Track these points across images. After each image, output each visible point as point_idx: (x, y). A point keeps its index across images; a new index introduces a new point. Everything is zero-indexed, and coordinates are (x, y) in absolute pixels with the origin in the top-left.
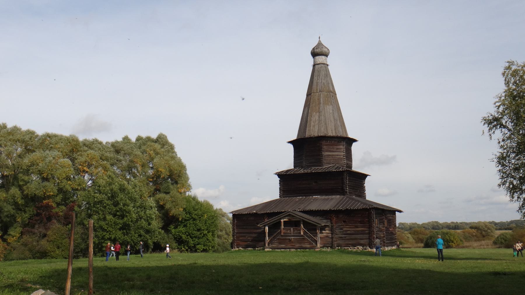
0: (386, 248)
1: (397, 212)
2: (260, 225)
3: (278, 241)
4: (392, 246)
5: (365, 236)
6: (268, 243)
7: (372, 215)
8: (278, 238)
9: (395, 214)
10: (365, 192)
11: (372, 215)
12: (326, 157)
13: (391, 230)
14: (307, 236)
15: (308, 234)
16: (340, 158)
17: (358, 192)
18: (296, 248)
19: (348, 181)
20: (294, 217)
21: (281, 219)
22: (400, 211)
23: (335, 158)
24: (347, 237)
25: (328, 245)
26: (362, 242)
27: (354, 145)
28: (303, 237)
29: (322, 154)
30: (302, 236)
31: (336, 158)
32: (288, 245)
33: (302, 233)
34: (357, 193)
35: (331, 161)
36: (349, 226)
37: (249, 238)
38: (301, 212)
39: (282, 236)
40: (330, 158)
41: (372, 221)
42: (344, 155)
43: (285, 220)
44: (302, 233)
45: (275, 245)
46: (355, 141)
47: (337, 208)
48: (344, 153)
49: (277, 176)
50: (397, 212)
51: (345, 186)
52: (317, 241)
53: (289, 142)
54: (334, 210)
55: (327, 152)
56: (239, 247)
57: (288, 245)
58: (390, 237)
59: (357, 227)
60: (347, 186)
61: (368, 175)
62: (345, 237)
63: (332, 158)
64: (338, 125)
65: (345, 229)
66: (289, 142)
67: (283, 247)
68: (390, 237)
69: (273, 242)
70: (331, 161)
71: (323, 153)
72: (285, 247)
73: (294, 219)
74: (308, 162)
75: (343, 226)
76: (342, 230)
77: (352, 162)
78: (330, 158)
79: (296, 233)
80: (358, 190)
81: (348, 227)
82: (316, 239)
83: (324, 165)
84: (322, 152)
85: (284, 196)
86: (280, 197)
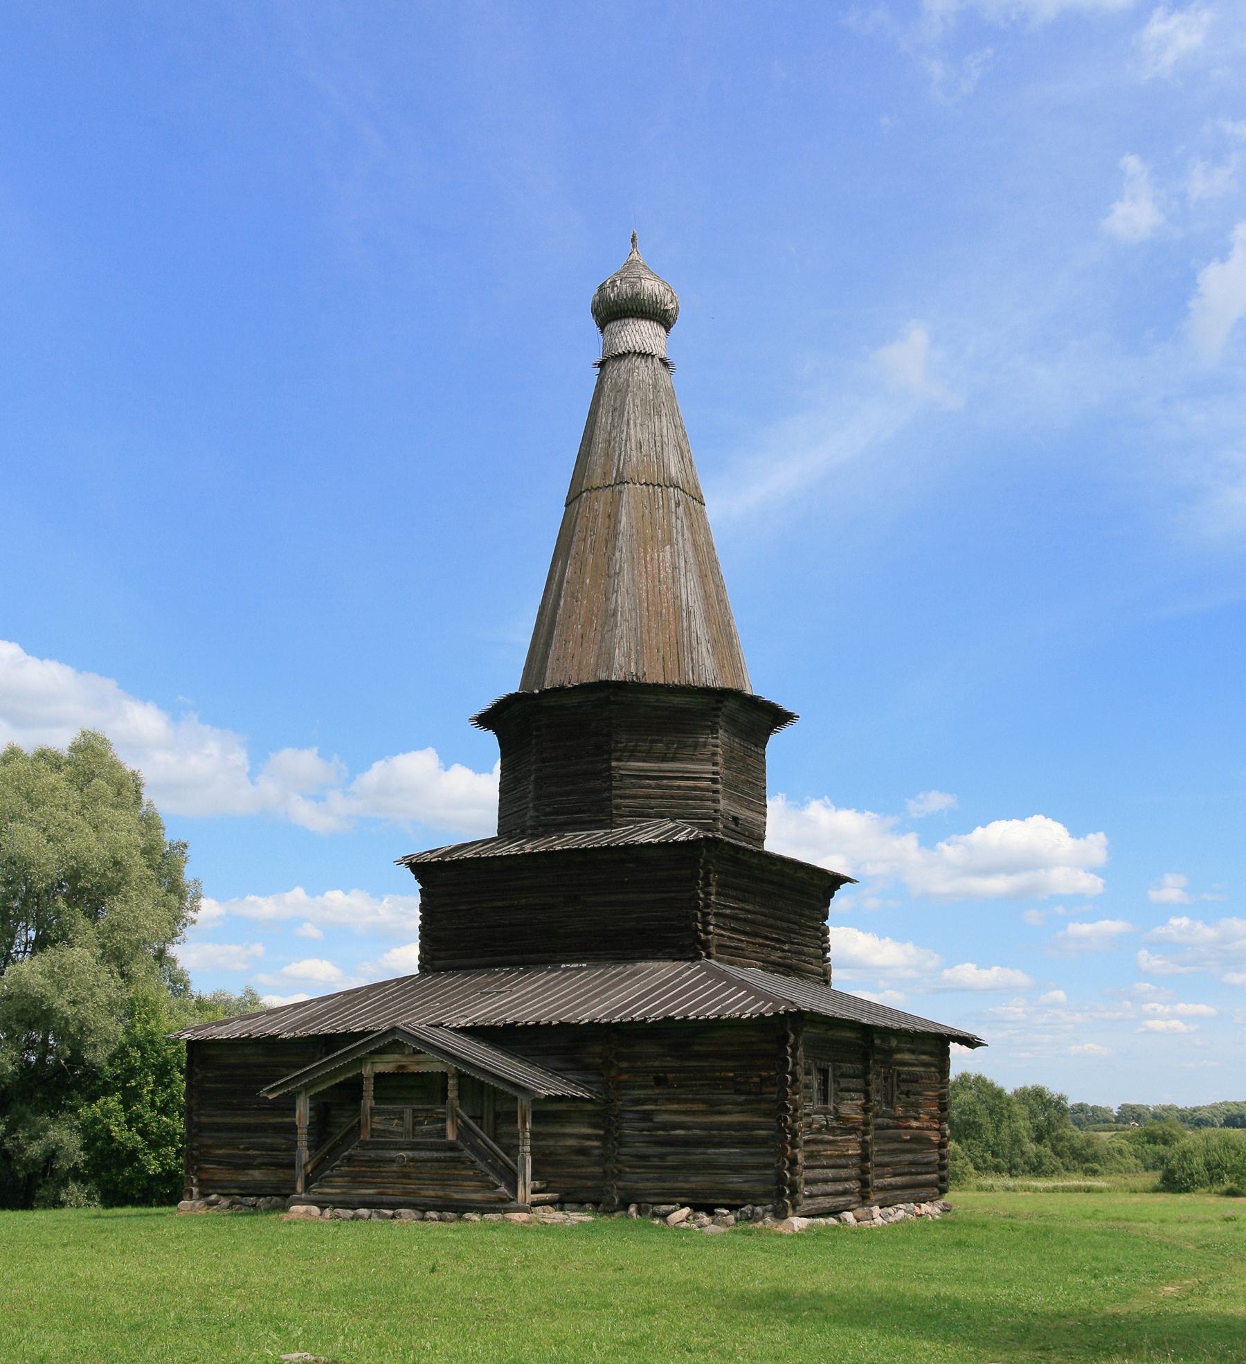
0: (876, 1210)
1: (954, 1048)
2: (271, 1091)
3: (347, 1169)
4: (920, 1201)
5: (753, 1154)
6: (307, 1176)
7: (789, 1050)
8: (346, 1153)
9: (944, 1054)
10: (828, 955)
11: (789, 1050)
12: (628, 781)
13: (914, 1124)
14: (474, 1149)
15: (479, 1136)
16: (695, 788)
17: (783, 951)
18: (425, 1205)
19: (713, 890)
20: (421, 1057)
21: (360, 1062)
22: (970, 1042)
23: (672, 787)
24: (670, 1158)
25: (581, 1196)
26: (736, 1181)
27: (778, 744)
28: (456, 1154)
29: (610, 768)
30: (452, 1147)
31: (679, 787)
32: (390, 1191)
33: (451, 1136)
34: (779, 954)
35: (653, 802)
36: (679, 1101)
37: (251, 1152)
38: (463, 1031)
39: (364, 1145)
40: (649, 787)
41: (789, 1077)
42: (714, 773)
43: (381, 1068)
44: (451, 1136)
45: (332, 1187)
46: (779, 717)
47: (625, 1016)
48: (715, 764)
49: (409, 875)
50: (954, 1048)
51: (699, 914)
52: (515, 1176)
53: (485, 720)
54: (608, 1024)
55: (632, 757)
56: (210, 1191)
57: (390, 1191)
58: (909, 1157)
59: (714, 1107)
60: (708, 914)
61: (846, 880)
62: (662, 1157)
63: (659, 787)
64: (694, 635)
65: (660, 1118)
66: (485, 720)
67: (367, 1199)
68: (909, 1157)
69: (328, 1172)
70: (653, 802)
71: (614, 764)
72: (377, 1199)
73: (418, 1063)
74: (548, 810)
75: (655, 1101)
76: (649, 1124)
77: (765, 815)
78: (649, 787)
79: (428, 1134)
80: (784, 943)
81: (675, 1107)
82: (511, 1163)
83: (619, 820)
84: (608, 761)
85: (438, 963)
86: (420, 967)
